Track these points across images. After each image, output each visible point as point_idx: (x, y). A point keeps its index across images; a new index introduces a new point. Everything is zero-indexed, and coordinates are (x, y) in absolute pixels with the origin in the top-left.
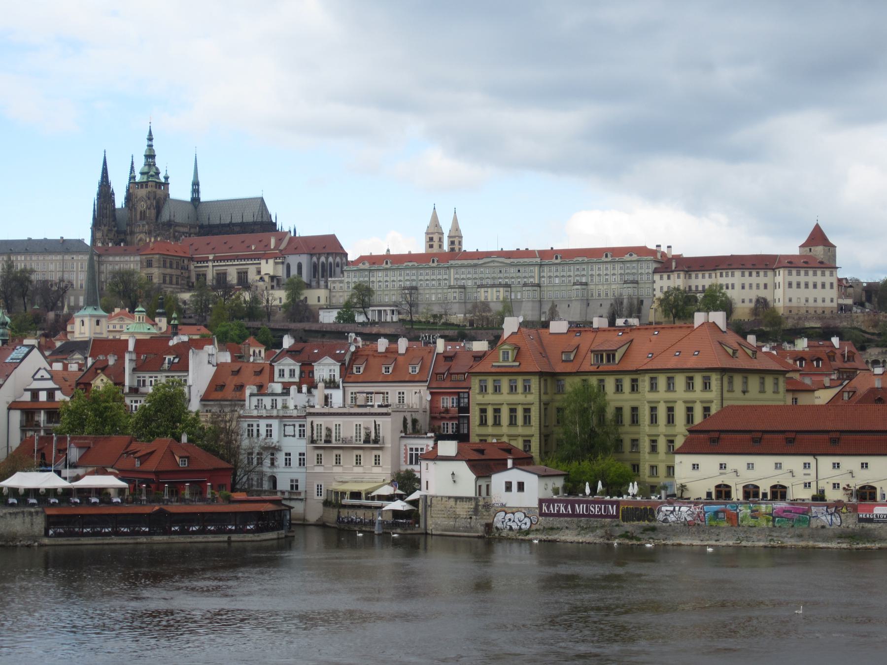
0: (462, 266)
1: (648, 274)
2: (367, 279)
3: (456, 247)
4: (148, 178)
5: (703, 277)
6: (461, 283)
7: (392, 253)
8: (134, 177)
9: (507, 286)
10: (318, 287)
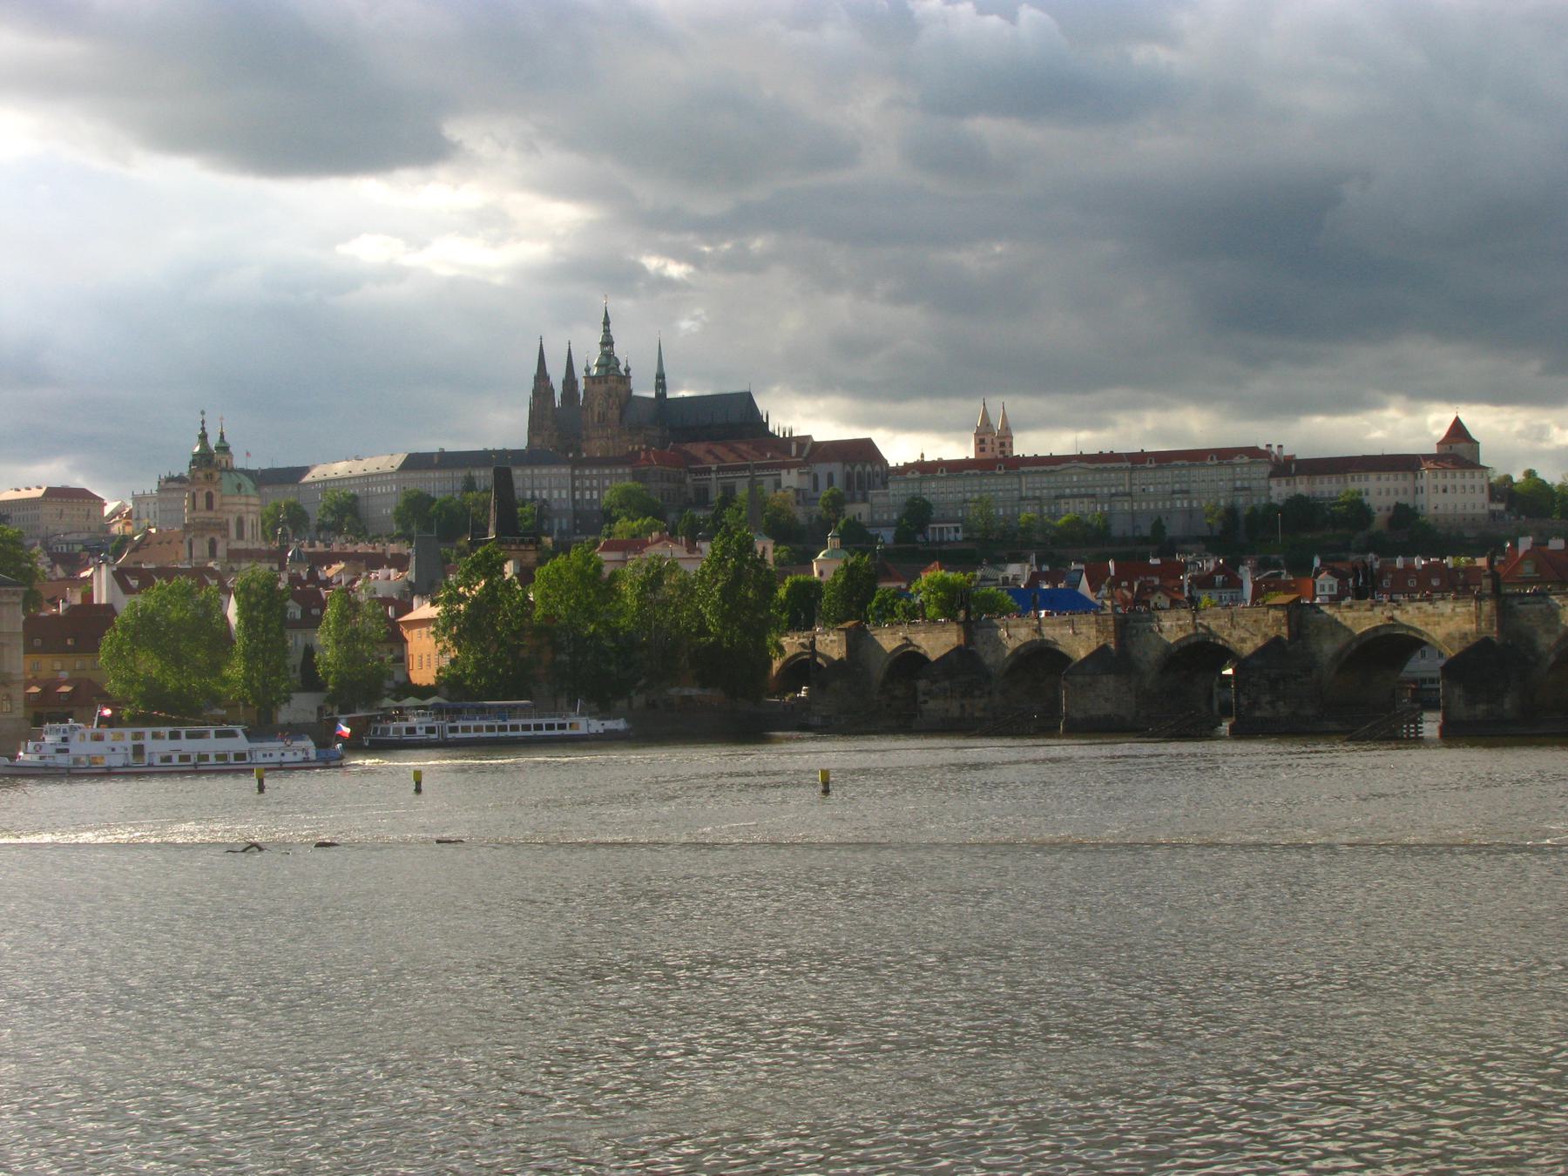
0: (1036, 472)
1: (1263, 478)
2: (917, 491)
3: (1007, 449)
4: (608, 371)
5: (1330, 482)
6: (1038, 493)
7: (927, 459)
8: (588, 370)
9: (1093, 496)
10: (853, 501)
